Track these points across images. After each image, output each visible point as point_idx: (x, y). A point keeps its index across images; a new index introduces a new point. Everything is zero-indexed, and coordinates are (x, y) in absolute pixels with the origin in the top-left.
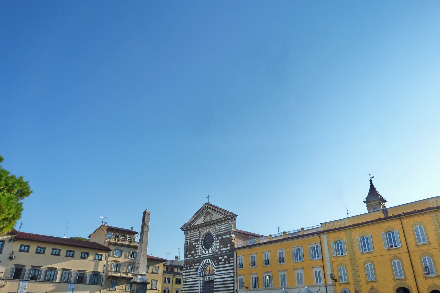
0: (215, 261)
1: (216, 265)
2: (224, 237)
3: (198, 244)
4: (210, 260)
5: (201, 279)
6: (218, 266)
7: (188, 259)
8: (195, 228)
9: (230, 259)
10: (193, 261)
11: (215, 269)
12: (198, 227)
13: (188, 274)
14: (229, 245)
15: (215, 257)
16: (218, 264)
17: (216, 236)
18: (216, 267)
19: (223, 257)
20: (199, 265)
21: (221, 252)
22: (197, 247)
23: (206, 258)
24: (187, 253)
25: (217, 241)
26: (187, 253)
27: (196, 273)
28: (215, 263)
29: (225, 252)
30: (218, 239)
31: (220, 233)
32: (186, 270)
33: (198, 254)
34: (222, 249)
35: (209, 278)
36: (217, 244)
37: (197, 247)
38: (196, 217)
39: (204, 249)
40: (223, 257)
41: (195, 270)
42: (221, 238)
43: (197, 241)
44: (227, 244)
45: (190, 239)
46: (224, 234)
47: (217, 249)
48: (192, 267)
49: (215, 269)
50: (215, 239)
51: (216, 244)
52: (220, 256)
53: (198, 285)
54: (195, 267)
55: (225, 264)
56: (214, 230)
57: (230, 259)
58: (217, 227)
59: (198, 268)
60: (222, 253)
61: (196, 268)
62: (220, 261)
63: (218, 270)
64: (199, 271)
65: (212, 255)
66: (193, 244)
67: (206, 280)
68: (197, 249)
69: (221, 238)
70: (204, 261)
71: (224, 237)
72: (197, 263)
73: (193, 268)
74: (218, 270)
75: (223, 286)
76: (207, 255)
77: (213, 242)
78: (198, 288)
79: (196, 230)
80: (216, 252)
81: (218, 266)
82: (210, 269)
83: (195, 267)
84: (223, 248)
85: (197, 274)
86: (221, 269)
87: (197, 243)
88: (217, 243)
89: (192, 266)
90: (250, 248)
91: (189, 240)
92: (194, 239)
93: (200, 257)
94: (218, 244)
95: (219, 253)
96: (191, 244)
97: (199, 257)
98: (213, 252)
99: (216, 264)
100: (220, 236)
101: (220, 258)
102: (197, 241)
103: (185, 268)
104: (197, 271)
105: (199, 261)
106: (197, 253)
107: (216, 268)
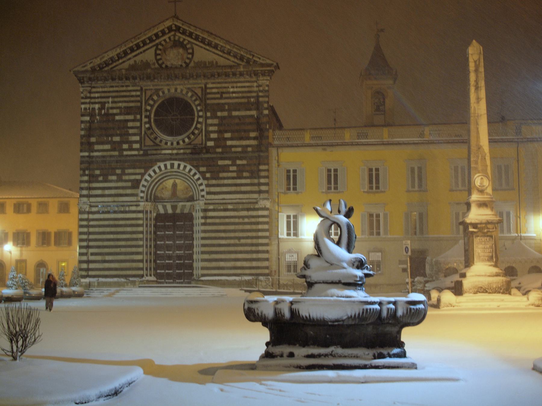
0: (203, 169)
1: (205, 178)
2: (235, 113)
4: (182, 164)
5: (148, 209)
6: (214, 182)
7: (95, 154)
8: (127, 79)
11: (201, 188)
14: (253, 134)
20: (143, 175)
22: (132, 128)
24: (93, 140)
25: (216, 121)
26: (93, 140)
27: (129, 191)
28: (203, 174)
30: (214, 116)
31: (223, 101)
32: (89, 182)
34: (229, 143)
35: (174, 208)
37: (132, 128)
41: (129, 184)
43: (128, 111)
49: (201, 188)
52: (222, 159)
53: (140, 222)
62: (225, 169)
63: (213, 189)
66: (117, 118)
67: (162, 211)
68: (131, 131)
69: (225, 114)
70: (162, 165)
71: (235, 113)
73: (120, 180)
74: (213, 189)
78: (140, 229)
79: (128, 83)
84: (231, 139)
86: (224, 189)
87: (131, 117)
89: (114, 174)
90: (325, 150)
91: (97, 106)
92: (120, 105)
94: (215, 128)
96: (108, 117)
100: (222, 110)
101: (220, 163)
102: (128, 111)
103: (86, 178)
106: (131, 143)
107: (207, 186)
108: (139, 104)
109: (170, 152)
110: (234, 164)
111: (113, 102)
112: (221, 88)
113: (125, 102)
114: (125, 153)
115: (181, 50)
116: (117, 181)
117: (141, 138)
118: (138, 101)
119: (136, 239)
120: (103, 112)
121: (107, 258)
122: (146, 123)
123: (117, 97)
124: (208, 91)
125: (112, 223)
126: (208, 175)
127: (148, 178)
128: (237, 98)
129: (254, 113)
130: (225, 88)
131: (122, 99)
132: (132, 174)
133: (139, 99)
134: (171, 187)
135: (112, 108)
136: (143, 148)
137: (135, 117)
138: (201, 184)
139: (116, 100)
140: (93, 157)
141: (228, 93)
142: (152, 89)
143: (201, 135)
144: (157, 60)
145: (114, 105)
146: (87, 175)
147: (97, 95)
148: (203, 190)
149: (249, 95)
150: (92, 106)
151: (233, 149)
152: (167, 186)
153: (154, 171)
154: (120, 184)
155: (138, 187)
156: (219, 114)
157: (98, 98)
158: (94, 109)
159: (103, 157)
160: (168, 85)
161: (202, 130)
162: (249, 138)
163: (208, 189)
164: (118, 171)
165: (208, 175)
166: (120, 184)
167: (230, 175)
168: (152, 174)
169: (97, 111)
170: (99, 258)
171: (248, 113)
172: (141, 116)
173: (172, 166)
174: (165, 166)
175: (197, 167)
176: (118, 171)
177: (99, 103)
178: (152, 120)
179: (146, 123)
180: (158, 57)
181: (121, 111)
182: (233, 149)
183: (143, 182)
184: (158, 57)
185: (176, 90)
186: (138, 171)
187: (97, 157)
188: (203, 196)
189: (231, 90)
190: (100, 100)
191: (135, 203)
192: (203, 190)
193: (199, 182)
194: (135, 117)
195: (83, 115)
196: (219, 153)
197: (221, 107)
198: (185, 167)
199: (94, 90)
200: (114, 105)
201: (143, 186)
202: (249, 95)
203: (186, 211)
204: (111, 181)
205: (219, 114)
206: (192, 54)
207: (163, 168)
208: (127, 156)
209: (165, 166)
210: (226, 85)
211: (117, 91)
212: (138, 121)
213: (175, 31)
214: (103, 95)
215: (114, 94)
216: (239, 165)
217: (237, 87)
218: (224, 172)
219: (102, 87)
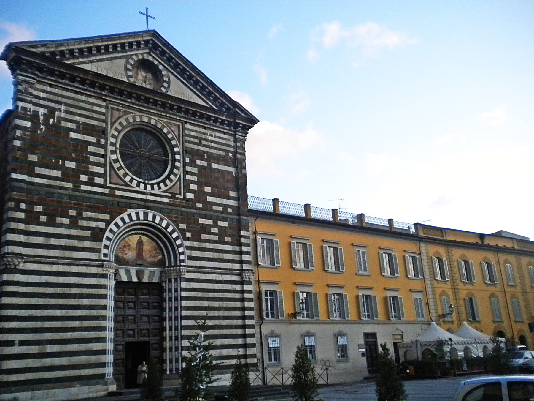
0: (183, 226)
2: (214, 166)
3: (98, 144)
6: (195, 244)
10: (71, 197)
11: (181, 250)
12: (112, 90)
13: (40, 240)
15: (182, 212)
16: (196, 238)
17: (186, 151)
20: (108, 223)
21: (208, 206)
23: (146, 205)
24: (33, 158)
25: (195, 170)
26: (33, 158)
27: (87, 244)
28: (183, 232)
29: (220, 209)
30: (193, 163)
33: (98, 180)
34: (210, 199)
35: (139, 274)
36: (188, 177)
38: (98, 49)
41: (88, 233)
43: (87, 129)
44: (227, 190)
46: (218, 159)
49: (181, 250)
52: (205, 217)
55: (221, 241)
56: (175, 129)
58: (188, 126)
59: (102, 231)
60: (211, 210)
62: (205, 229)
64: (105, 242)
65: (168, 204)
66: (73, 135)
67: (125, 278)
68: (92, 159)
69: (205, 164)
71: (214, 166)
73: (73, 224)
75: (216, 304)
76: (150, 198)
81: (195, 244)
82: (140, 243)
84: (212, 195)
85: (98, 251)
86: (207, 255)
87: (93, 140)
89: (65, 215)
94: (195, 179)
95: (200, 205)
96: (58, 131)
97: (107, 191)
98: (173, 196)
100: (202, 159)
101: (202, 221)
102: (87, 129)
103: (22, 215)
105: (114, 207)
106: (93, 175)
108: (104, 125)
109: (143, 197)
110: (215, 225)
111: (66, 112)
114: (83, 187)
117: (105, 171)
120: (51, 121)
121: (49, 349)
124: (186, 132)
125: (59, 290)
126: (188, 235)
127: (115, 229)
128: (215, 148)
131: (80, 112)
132: (93, 219)
133: (103, 117)
134: (135, 246)
136: (108, 185)
137: (98, 141)
138: (181, 245)
139: (71, 109)
140: (32, 184)
141: (206, 140)
142: (118, 110)
143: (178, 183)
144: (129, 77)
145: (69, 117)
146: (22, 211)
147: (42, 95)
148: (182, 253)
150: (36, 109)
151: (214, 208)
152: (131, 243)
153: (123, 219)
154: (74, 232)
155: (101, 241)
156: (198, 162)
157: (44, 99)
158: (36, 115)
160: (140, 111)
161: (180, 176)
162: (229, 198)
163: (188, 253)
164: (72, 213)
165: (188, 235)
166: (74, 232)
167: (212, 237)
168: (120, 223)
169: (42, 118)
170: (34, 349)
171: (227, 168)
172: (106, 143)
173: (146, 215)
174: (137, 214)
175: (176, 223)
176: (72, 213)
177: (44, 106)
180: (130, 73)
181: (78, 127)
182: (214, 208)
183: (107, 234)
184: (130, 73)
185: (150, 119)
186: (101, 216)
187: (39, 185)
188: (183, 261)
189: (210, 138)
190: (46, 103)
192: (182, 253)
193: (178, 242)
194: (98, 141)
197: (200, 155)
198: (162, 220)
199: (39, 86)
200: (69, 117)
201: (108, 239)
203: (155, 280)
204: (61, 225)
207: (134, 218)
208: (85, 191)
209: (137, 214)
210: (204, 131)
211: (73, 99)
212: (102, 146)
213: (150, 49)
214: (51, 97)
215: (69, 101)
216: (221, 227)
217: (215, 137)
219: (51, 86)
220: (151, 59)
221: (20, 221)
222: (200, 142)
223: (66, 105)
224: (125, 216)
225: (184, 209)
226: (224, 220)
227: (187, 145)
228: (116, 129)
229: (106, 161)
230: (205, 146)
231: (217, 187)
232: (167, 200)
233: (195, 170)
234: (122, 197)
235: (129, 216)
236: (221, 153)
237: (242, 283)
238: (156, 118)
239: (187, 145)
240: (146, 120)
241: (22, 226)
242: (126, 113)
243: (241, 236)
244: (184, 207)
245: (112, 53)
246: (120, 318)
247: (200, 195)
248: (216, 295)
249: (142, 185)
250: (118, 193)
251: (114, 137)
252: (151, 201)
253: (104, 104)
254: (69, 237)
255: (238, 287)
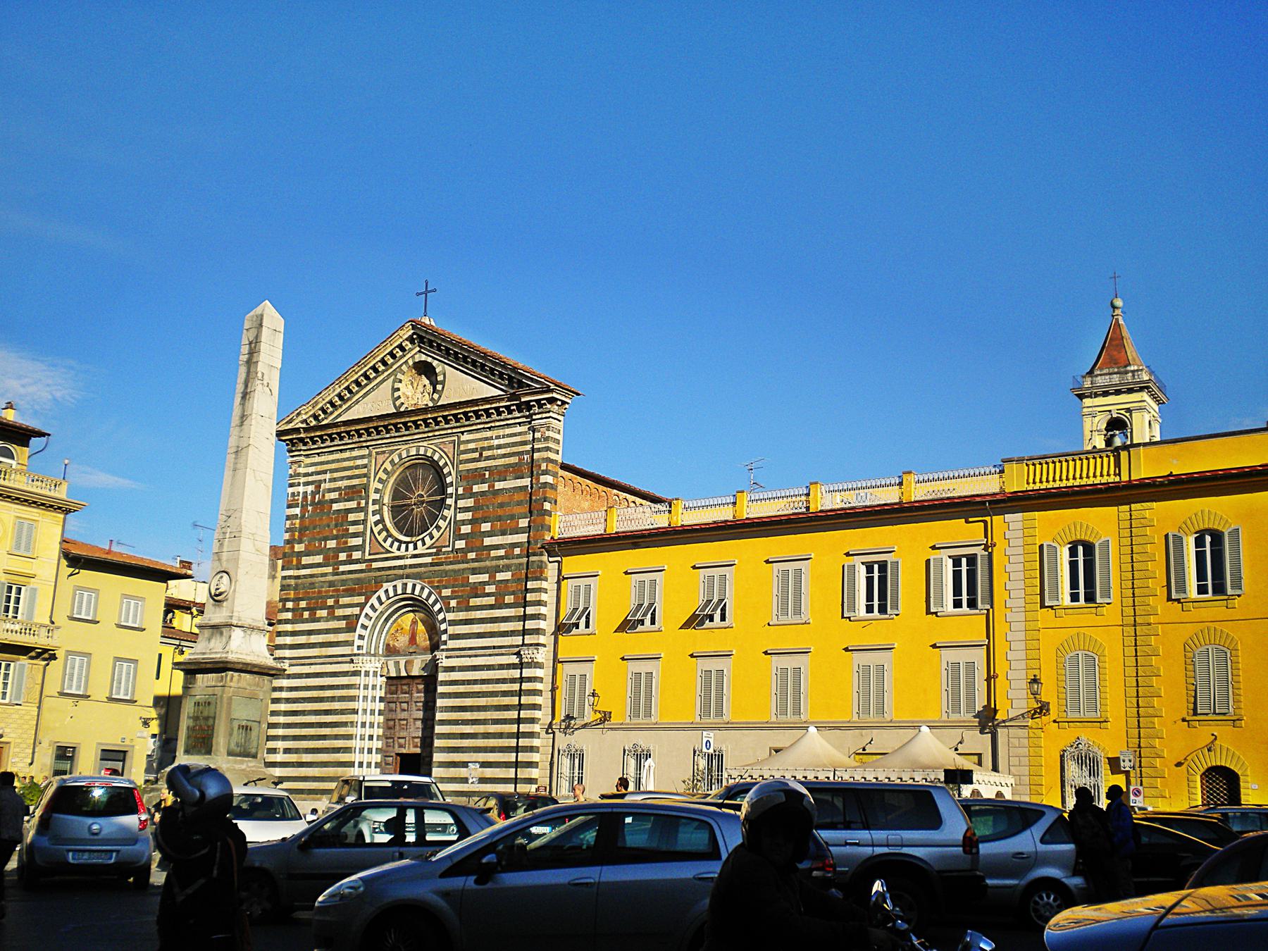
0: (446, 592)
2: (498, 485)
3: (359, 509)
6: (462, 615)
9: (530, 585)
10: (331, 584)
11: (443, 627)
14: (523, 523)
15: (446, 572)
18: (450, 616)
19: (492, 577)
20: (362, 606)
22: (355, 523)
25: (470, 502)
27: (342, 637)
29: (502, 552)
30: (469, 493)
33: (356, 555)
34: (488, 541)
36: (460, 516)
37: (355, 523)
39: (390, 535)
40: (492, 577)
41: (343, 624)
42: (485, 487)
43: (352, 493)
45: (318, 484)
46: (502, 473)
47: (460, 537)
48: (324, 613)
49: (443, 627)
50: (450, 490)
51: (457, 510)
52: (475, 571)
54: (339, 612)
55: (499, 605)
57: (530, 585)
58: (465, 437)
59: (358, 617)
60: (488, 557)
61: (345, 617)
62: (477, 591)
64: (359, 630)
65: (432, 564)
66: (335, 507)
67: (393, 674)
68: (352, 529)
69: (485, 487)
70: (389, 586)
71: (498, 485)
72: (350, 592)
75: (482, 701)
77: (441, 504)
80: (457, 551)
81: (462, 615)
82: (414, 623)
83: (339, 612)
84: (490, 534)
85: (351, 643)
87: (353, 504)
88: (466, 509)
91: (310, 488)
93: (370, 570)
94: (468, 516)
96: (322, 506)
97: (363, 566)
99: (453, 603)
103: (289, 615)
104: (351, 628)
107: (453, 623)
112: (481, 440)
113: (349, 478)
114: (342, 568)
115: (427, 382)
116: (327, 620)
117: (364, 541)
118: (365, 475)
119: (344, 724)
122: (374, 513)
123: (336, 470)
124: (462, 447)
127: (371, 613)
128: (504, 456)
129: (526, 482)
130: (486, 439)
133: (365, 471)
135: (330, 490)
136: (367, 557)
137: (359, 504)
139: (336, 475)
141: (490, 448)
142: (384, 452)
145: (333, 485)
146: (288, 610)
149: (521, 449)
150: (301, 489)
153: (379, 598)
156: (476, 489)
159: (312, 576)
163: (451, 630)
164: (330, 602)
172: (367, 503)
178: (385, 508)
179: (374, 513)
182: (493, 553)
183: (362, 620)
188: (445, 643)
189: (496, 442)
191: (348, 659)
193: (441, 617)
194: (359, 504)
195: (289, 506)
196: (473, 560)
197: (477, 476)
198: (423, 589)
202: (521, 449)
204: (318, 620)
205: (476, 489)
206: (443, 383)
208: (343, 573)
209: (395, 586)
210: (489, 434)
211: (338, 461)
215: (333, 466)
218: (476, 596)
220: (424, 358)
221: (287, 622)
222: (481, 455)
223: (332, 471)
224: (381, 593)
225: (451, 567)
226: (507, 568)
227: (461, 467)
228: (380, 481)
229: (365, 528)
230: (488, 458)
231: (499, 519)
232: (428, 560)
233: (470, 502)
234: (379, 569)
235: (387, 591)
236: (514, 460)
237: (521, 666)
238: (425, 444)
239: (461, 467)
240: (413, 452)
241: (289, 627)
242: (392, 452)
243: (527, 590)
244: (451, 563)
245: (375, 378)
246: (391, 723)
247: (474, 540)
248: (484, 688)
249: (403, 546)
250: (375, 565)
251: (381, 490)
252: (411, 566)
253: (366, 452)
254: (327, 631)
255: (516, 673)
